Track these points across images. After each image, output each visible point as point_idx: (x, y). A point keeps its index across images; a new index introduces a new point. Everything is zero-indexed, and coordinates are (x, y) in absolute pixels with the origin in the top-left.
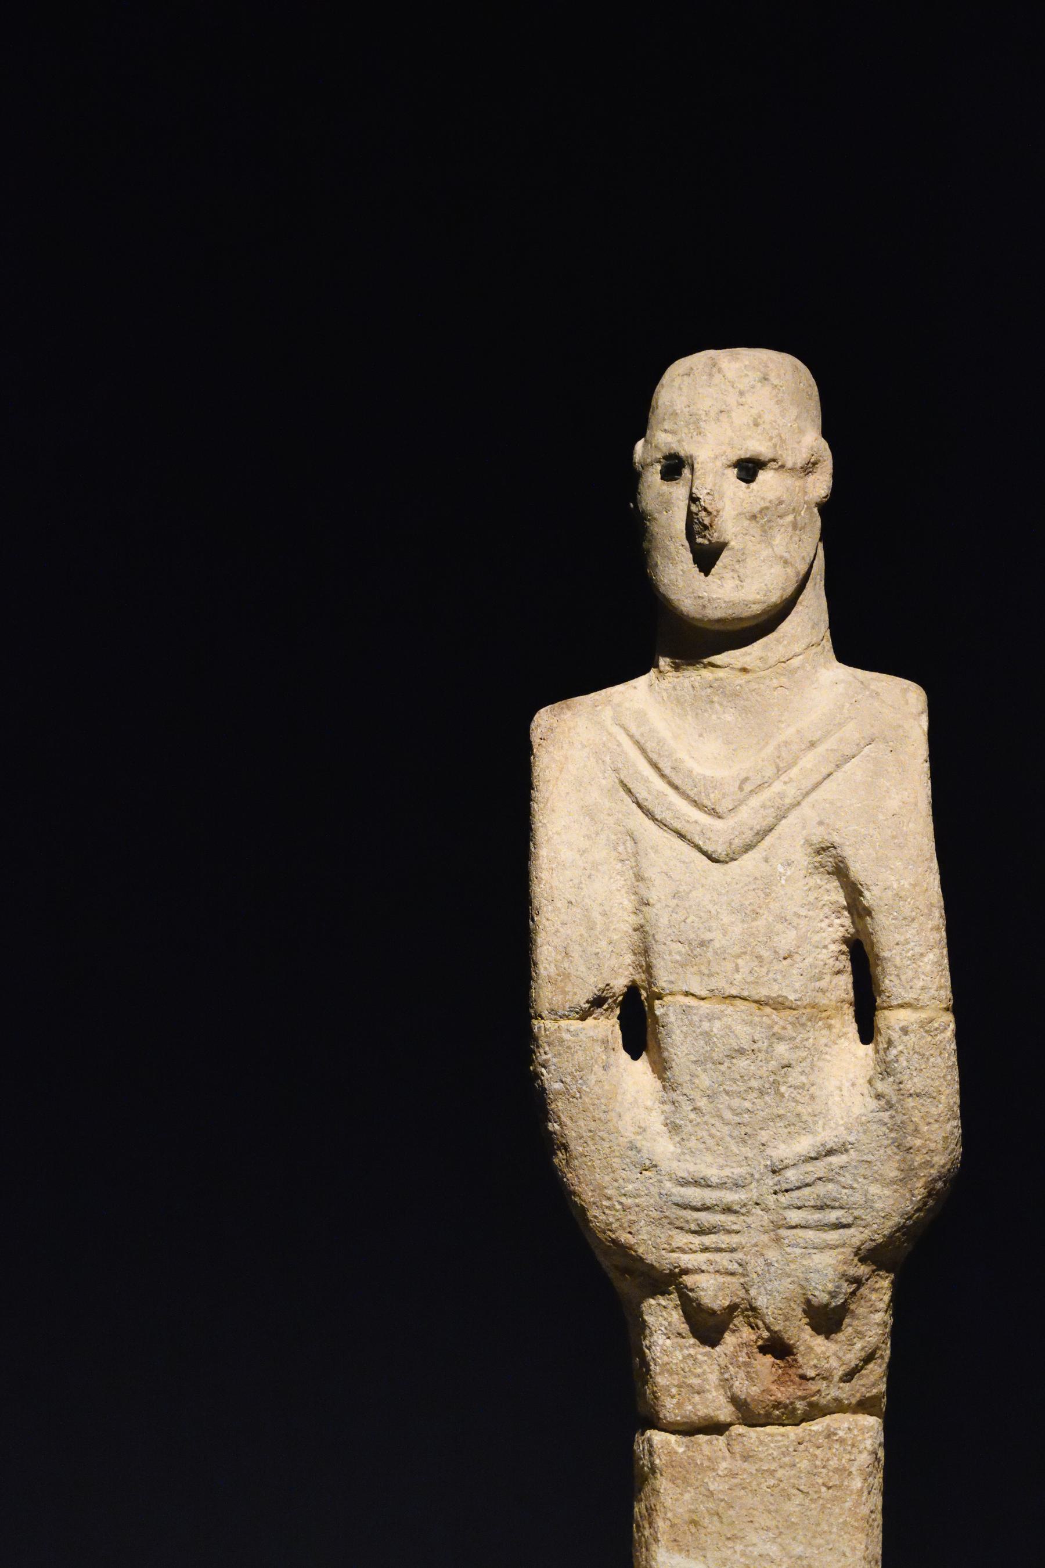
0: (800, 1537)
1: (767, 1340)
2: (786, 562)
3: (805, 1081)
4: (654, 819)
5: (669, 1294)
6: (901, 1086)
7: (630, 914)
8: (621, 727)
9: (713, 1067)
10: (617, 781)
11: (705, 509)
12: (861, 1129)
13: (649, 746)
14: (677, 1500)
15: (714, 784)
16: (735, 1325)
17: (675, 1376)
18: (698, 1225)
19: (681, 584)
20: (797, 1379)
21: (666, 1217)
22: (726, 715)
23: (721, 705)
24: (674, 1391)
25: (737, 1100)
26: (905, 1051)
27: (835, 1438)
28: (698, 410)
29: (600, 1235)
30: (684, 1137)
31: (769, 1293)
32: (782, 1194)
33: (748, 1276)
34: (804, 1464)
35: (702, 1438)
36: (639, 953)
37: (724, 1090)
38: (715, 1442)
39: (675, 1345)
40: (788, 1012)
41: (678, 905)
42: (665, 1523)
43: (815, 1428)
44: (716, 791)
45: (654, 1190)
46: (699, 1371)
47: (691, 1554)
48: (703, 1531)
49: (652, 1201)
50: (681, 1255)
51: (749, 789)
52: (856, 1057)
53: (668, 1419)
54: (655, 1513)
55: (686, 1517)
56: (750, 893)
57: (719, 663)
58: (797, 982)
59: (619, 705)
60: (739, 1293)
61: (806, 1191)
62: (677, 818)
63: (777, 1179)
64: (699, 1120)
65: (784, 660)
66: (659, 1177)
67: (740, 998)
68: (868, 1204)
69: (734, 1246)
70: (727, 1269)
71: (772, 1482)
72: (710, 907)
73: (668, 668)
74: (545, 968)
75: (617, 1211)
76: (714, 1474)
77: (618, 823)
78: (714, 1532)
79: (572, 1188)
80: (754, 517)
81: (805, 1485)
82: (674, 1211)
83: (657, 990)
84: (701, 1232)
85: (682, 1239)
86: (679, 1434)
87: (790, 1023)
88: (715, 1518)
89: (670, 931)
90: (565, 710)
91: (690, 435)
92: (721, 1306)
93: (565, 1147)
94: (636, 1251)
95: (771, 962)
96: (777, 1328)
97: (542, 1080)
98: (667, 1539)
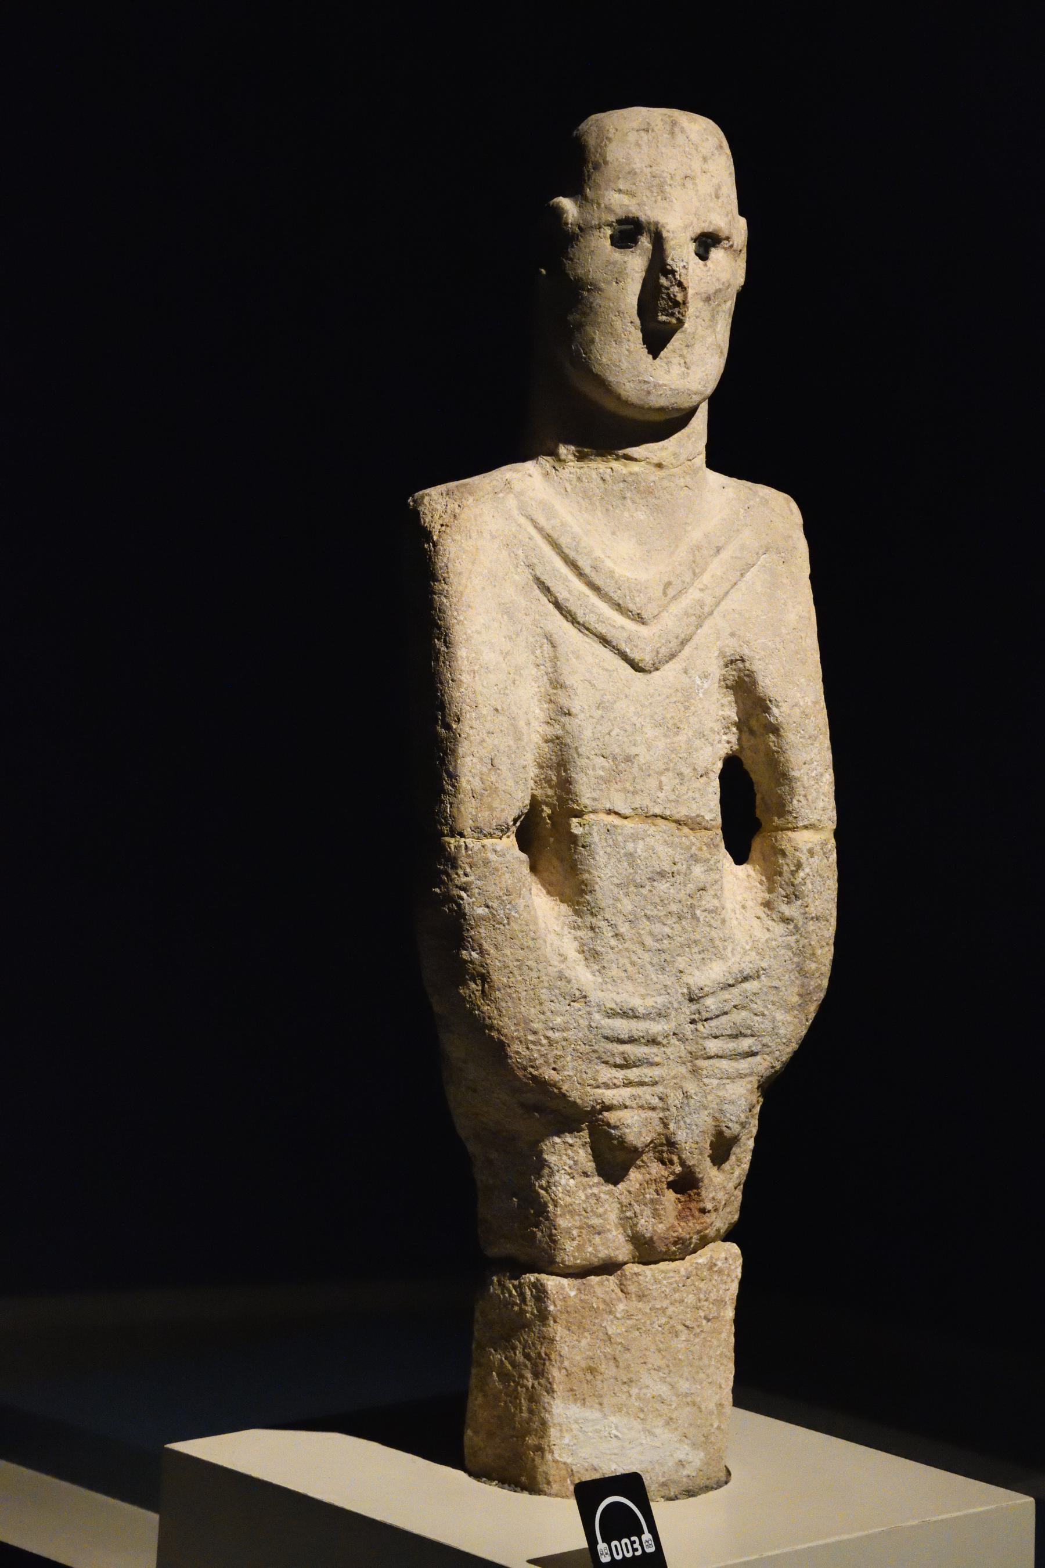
0: (686, 1374)
1: (678, 1175)
2: (721, 352)
3: (717, 905)
4: (573, 620)
5: (579, 1132)
6: (807, 909)
7: (541, 724)
8: (527, 518)
9: (635, 890)
10: (531, 578)
11: (680, 284)
12: (772, 954)
13: (564, 541)
14: (573, 1347)
15: (638, 587)
16: (643, 1161)
17: (577, 1218)
18: (624, 1058)
19: (625, 365)
20: (697, 1214)
21: (594, 1051)
22: (639, 513)
23: (633, 502)
24: (575, 1232)
25: (658, 925)
26: (811, 873)
27: (715, 1269)
28: (663, 171)
29: (520, 1073)
30: (606, 965)
31: (689, 1127)
32: (701, 1023)
33: (669, 1110)
34: (691, 1299)
35: (594, 1279)
36: (548, 767)
37: (645, 915)
38: (606, 1283)
39: (580, 1185)
40: (704, 832)
41: (602, 717)
42: (560, 1373)
43: (700, 1261)
44: (641, 595)
45: (584, 1023)
46: (601, 1210)
47: (587, 1403)
48: (599, 1377)
49: (580, 1035)
50: (604, 1091)
51: (672, 595)
52: (738, 879)
53: (567, 1263)
54: (547, 1363)
55: (583, 1364)
56: (671, 705)
57: (635, 456)
58: (712, 801)
59: (522, 493)
60: (657, 1128)
61: (724, 1019)
62: (601, 621)
63: (694, 1007)
64: (620, 947)
65: (691, 458)
66: (588, 1009)
67: (662, 817)
68: (774, 1032)
69: (657, 1079)
70: (650, 1104)
71: (663, 1320)
72: (634, 719)
73: (571, 457)
74: (469, 781)
75: (542, 1045)
76: (611, 1317)
77: (536, 623)
78: (612, 1377)
79: (488, 1021)
80: (708, 299)
81: (690, 1320)
82: (602, 1044)
83: (578, 808)
84: (626, 1065)
85: (607, 1074)
86: (572, 1278)
87: (705, 844)
88: (612, 1363)
89: (594, 744)
90: (466, 495)
91: (653, 199)
92: (644, 1142)
93: (485, 978)
94: (560, 1089)
95: (689, 781)
96: (690, 1163)
97: (459, 905)
98: (563, 1389)
